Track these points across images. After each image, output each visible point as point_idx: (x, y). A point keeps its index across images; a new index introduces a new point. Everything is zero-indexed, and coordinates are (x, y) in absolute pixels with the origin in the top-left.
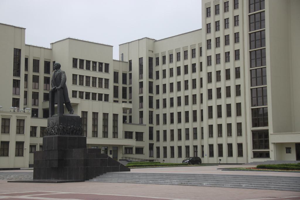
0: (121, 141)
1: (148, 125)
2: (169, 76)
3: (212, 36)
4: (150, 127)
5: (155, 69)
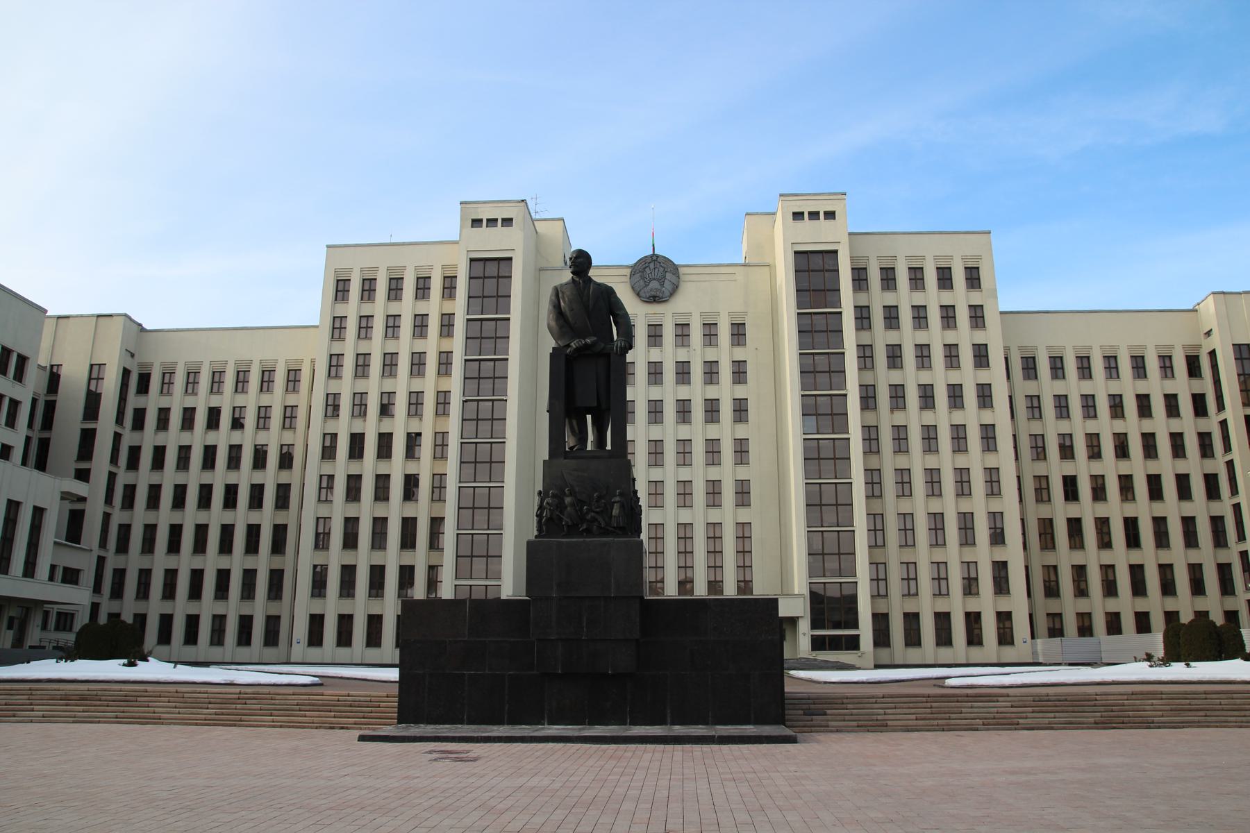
0: (40, 589)
1: (97, 551)
2: (154, 427)
3: (349, 347)
4: (99, 557)
5: (133, 401)
